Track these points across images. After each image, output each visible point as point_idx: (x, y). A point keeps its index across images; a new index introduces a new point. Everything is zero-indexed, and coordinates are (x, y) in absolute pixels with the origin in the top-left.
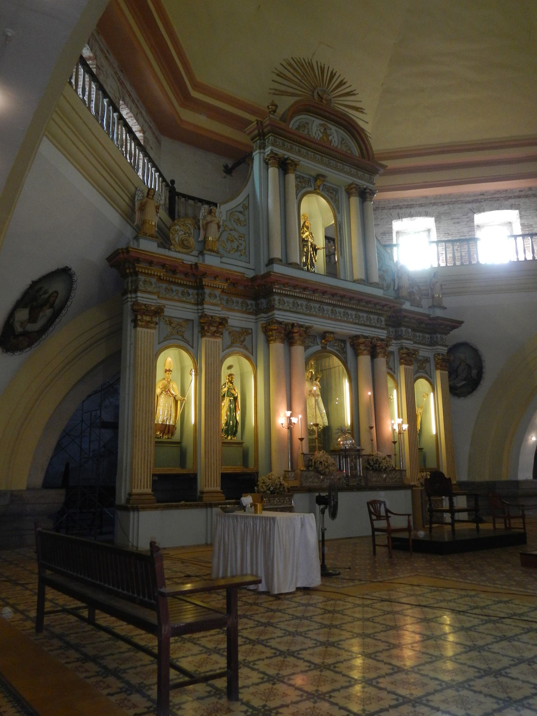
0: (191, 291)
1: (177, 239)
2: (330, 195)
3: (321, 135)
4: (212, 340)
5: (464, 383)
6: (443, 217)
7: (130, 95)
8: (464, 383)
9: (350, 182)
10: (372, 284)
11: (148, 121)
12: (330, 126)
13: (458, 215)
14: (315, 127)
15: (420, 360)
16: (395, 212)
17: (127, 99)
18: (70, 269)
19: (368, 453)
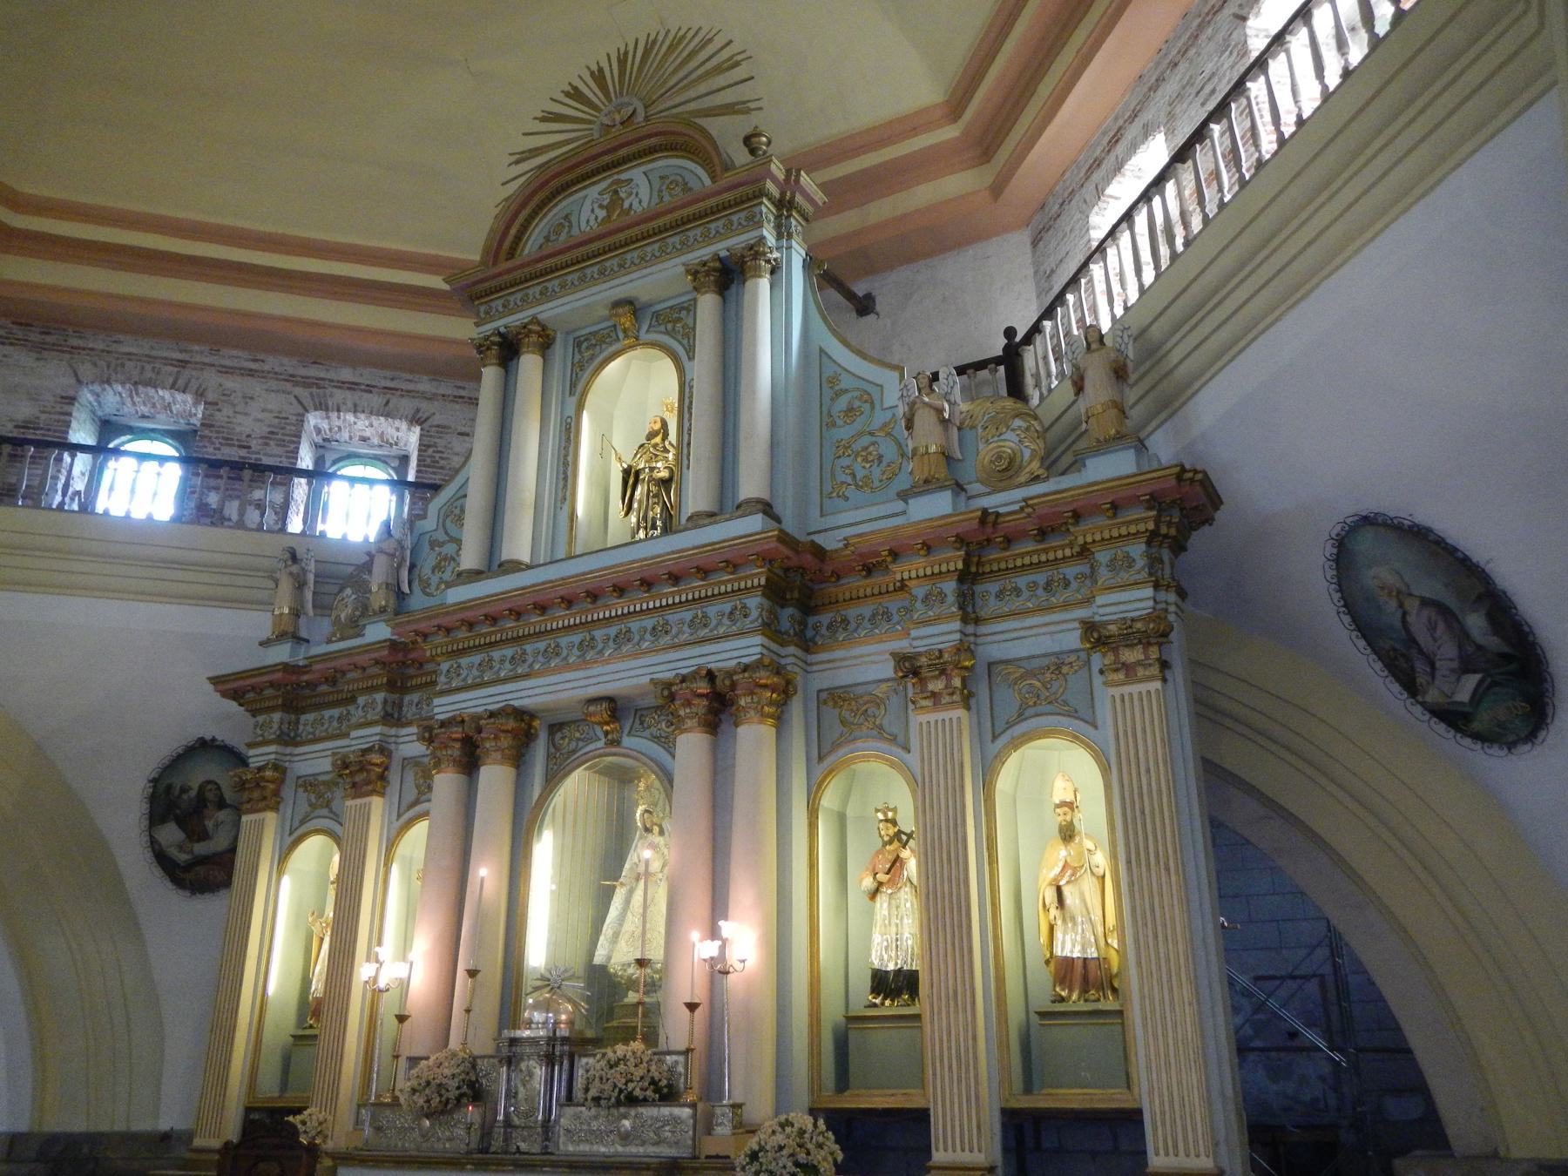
0: (351, 708)
1: (343, 617)
2: (669, 326)
3: (602, 214)
4: (358, 801)
5: (1471, 681)
6: (1178, 110)
7: (352, 386)
8: (1471, 681)
9: (682, 269)
10: (739, 507)
11: (449, 392)
12: (623, 176)
13: (1209, 68)
14: (586, 209)
15: (1031, 674)
16: (1090, 186)
17: (339, 395)
18: (214, 739)
19: (682, 1047)
